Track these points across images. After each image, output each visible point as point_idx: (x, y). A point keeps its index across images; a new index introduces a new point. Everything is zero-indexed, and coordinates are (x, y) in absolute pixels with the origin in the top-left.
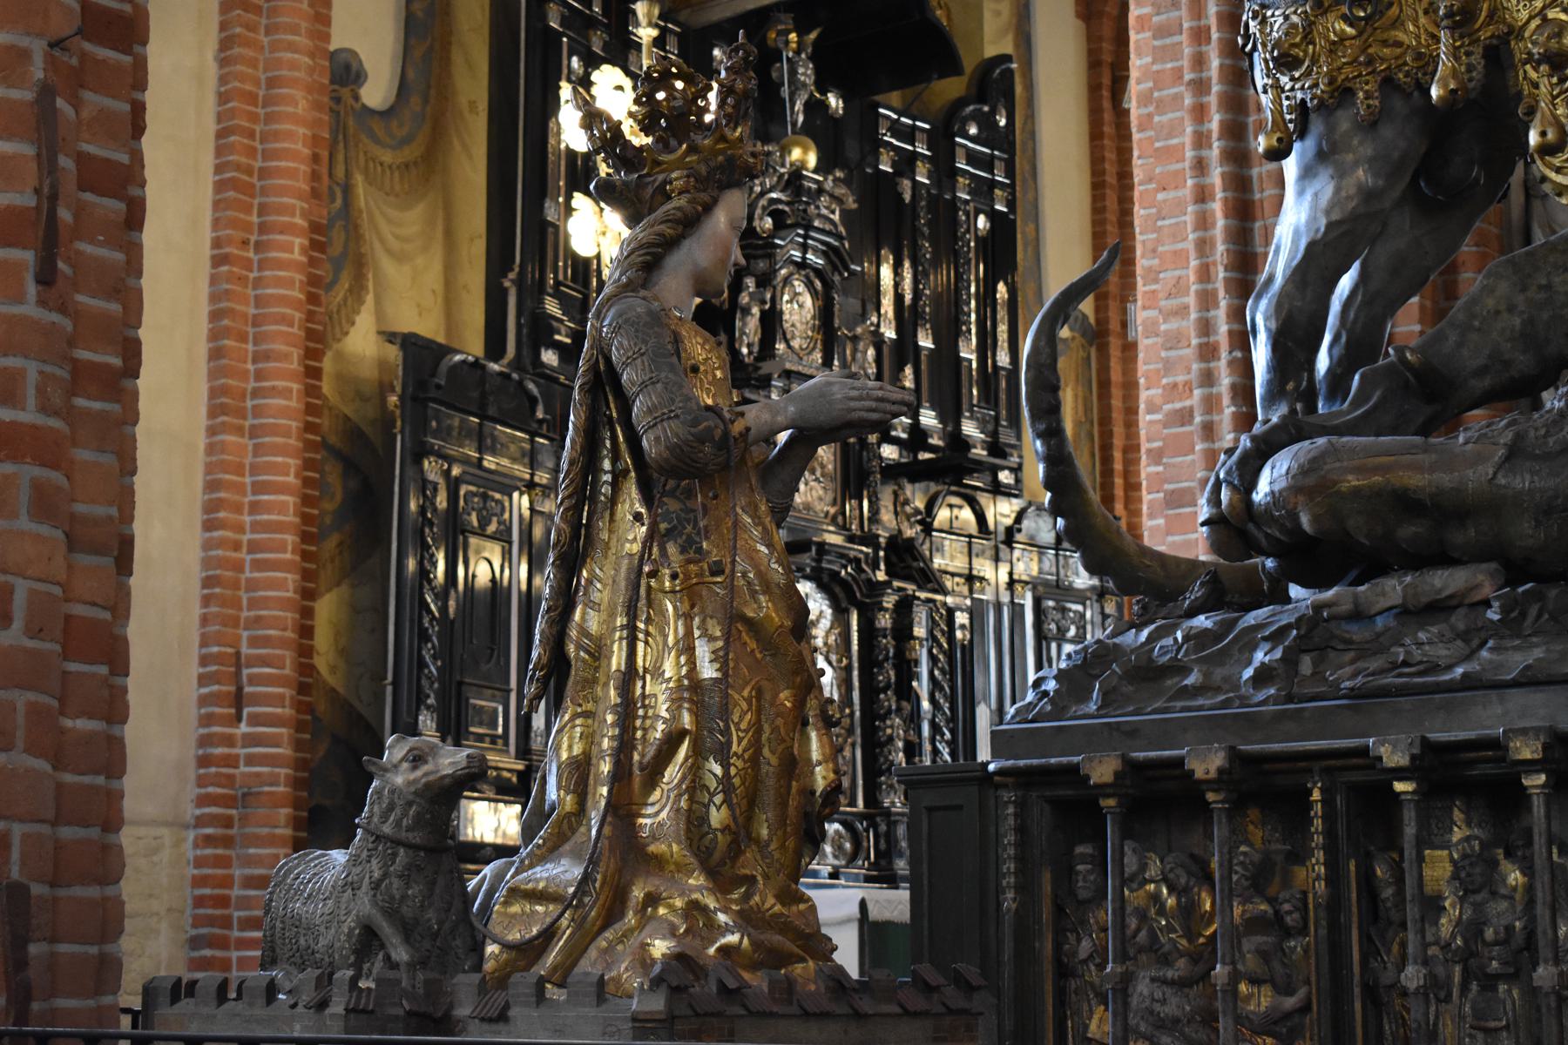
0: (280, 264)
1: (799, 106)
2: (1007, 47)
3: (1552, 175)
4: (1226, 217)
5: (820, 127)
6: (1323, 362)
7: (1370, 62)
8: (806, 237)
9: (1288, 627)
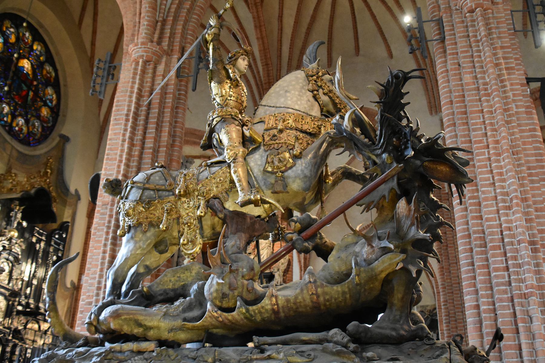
2: (69, 220)
3: (184, 251)
4: (109, 257)
5: (20, 228)
6: (124, 288)
7: (147, 218)
9: (103, 353)
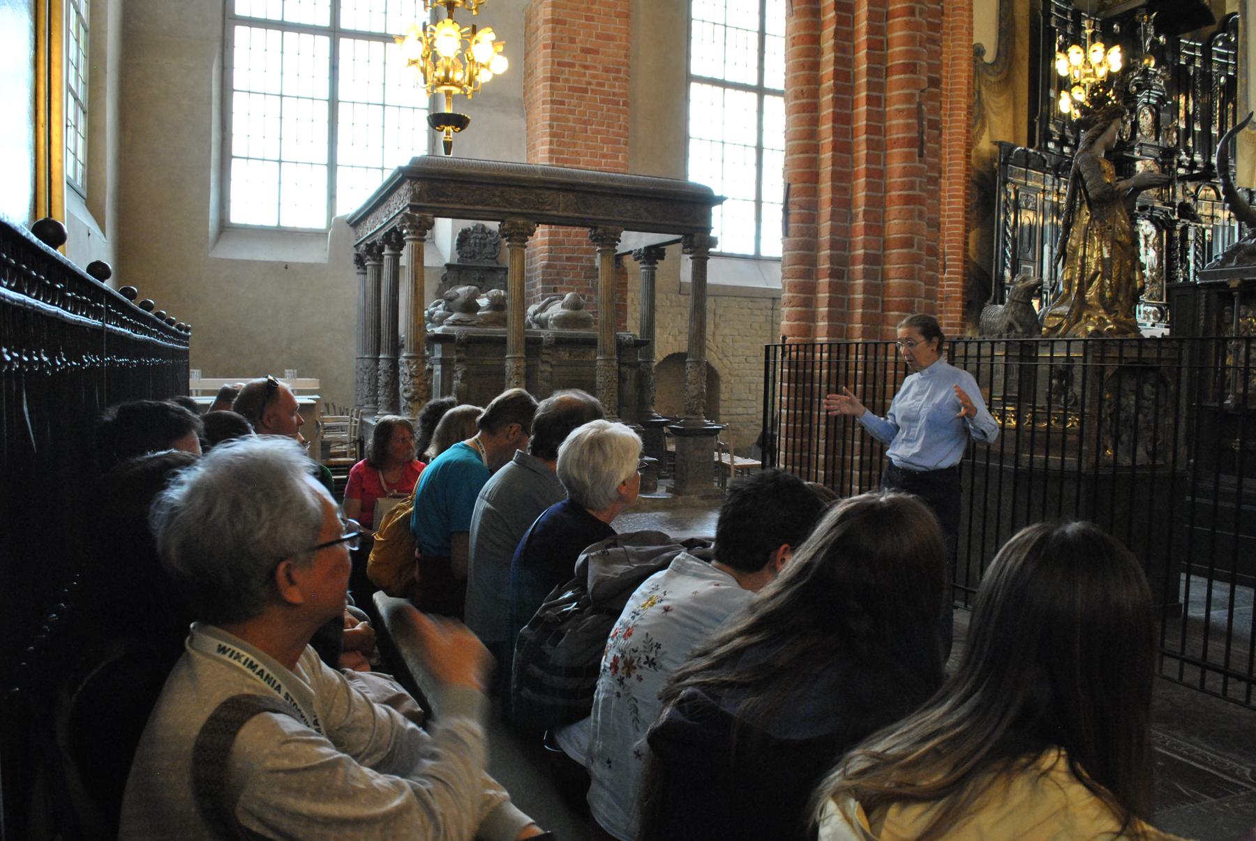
0: (957, 121)
1: (1147, 42)
2: (1236, 9)
5: (1157, 51)
8: (1149, 93)
